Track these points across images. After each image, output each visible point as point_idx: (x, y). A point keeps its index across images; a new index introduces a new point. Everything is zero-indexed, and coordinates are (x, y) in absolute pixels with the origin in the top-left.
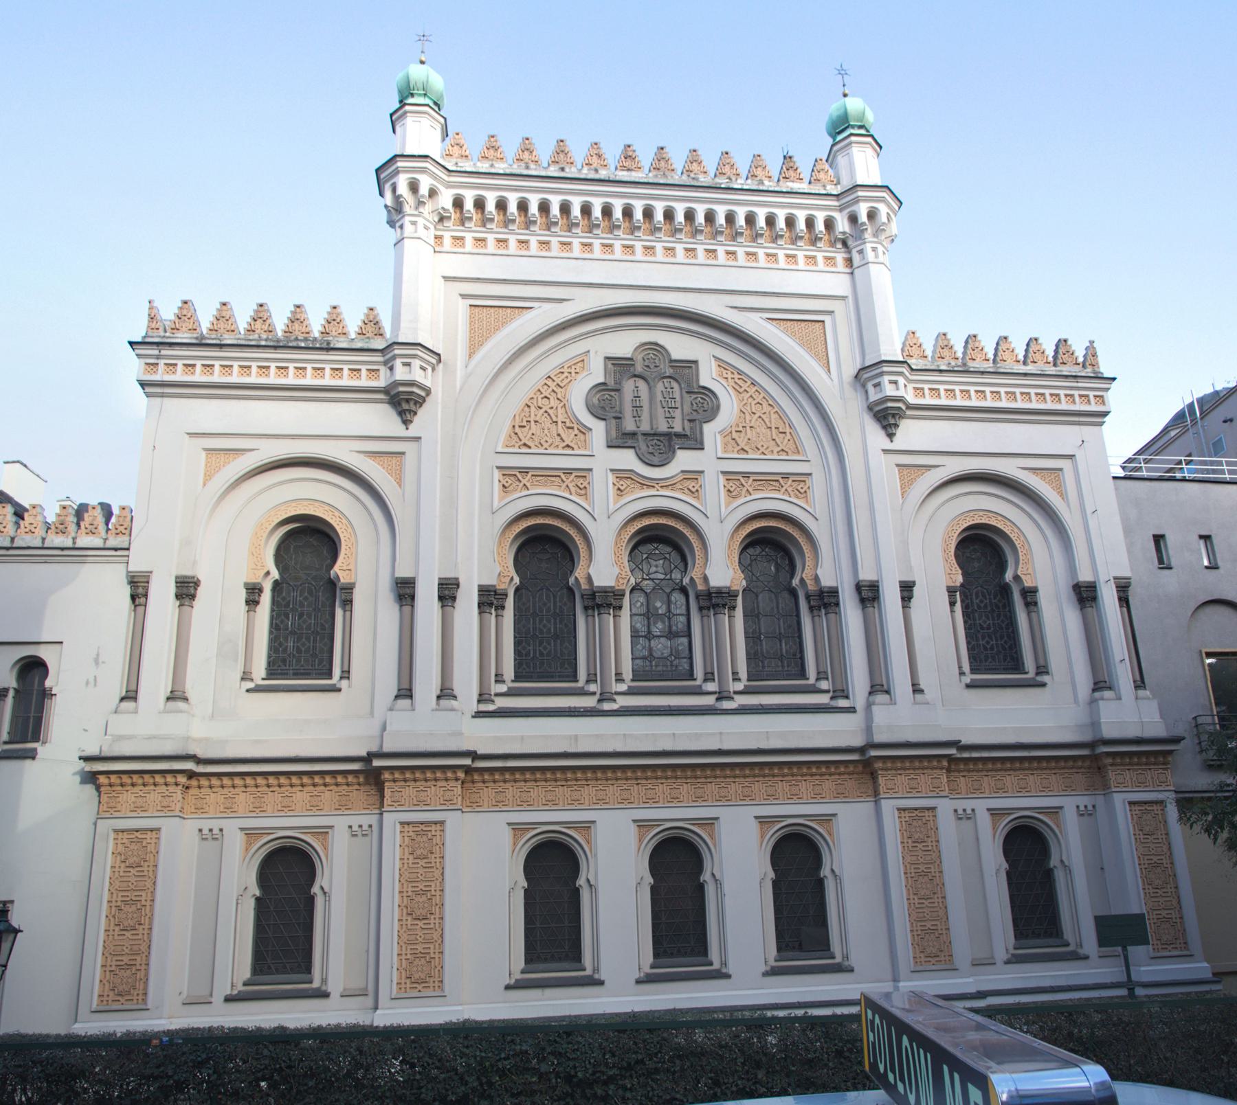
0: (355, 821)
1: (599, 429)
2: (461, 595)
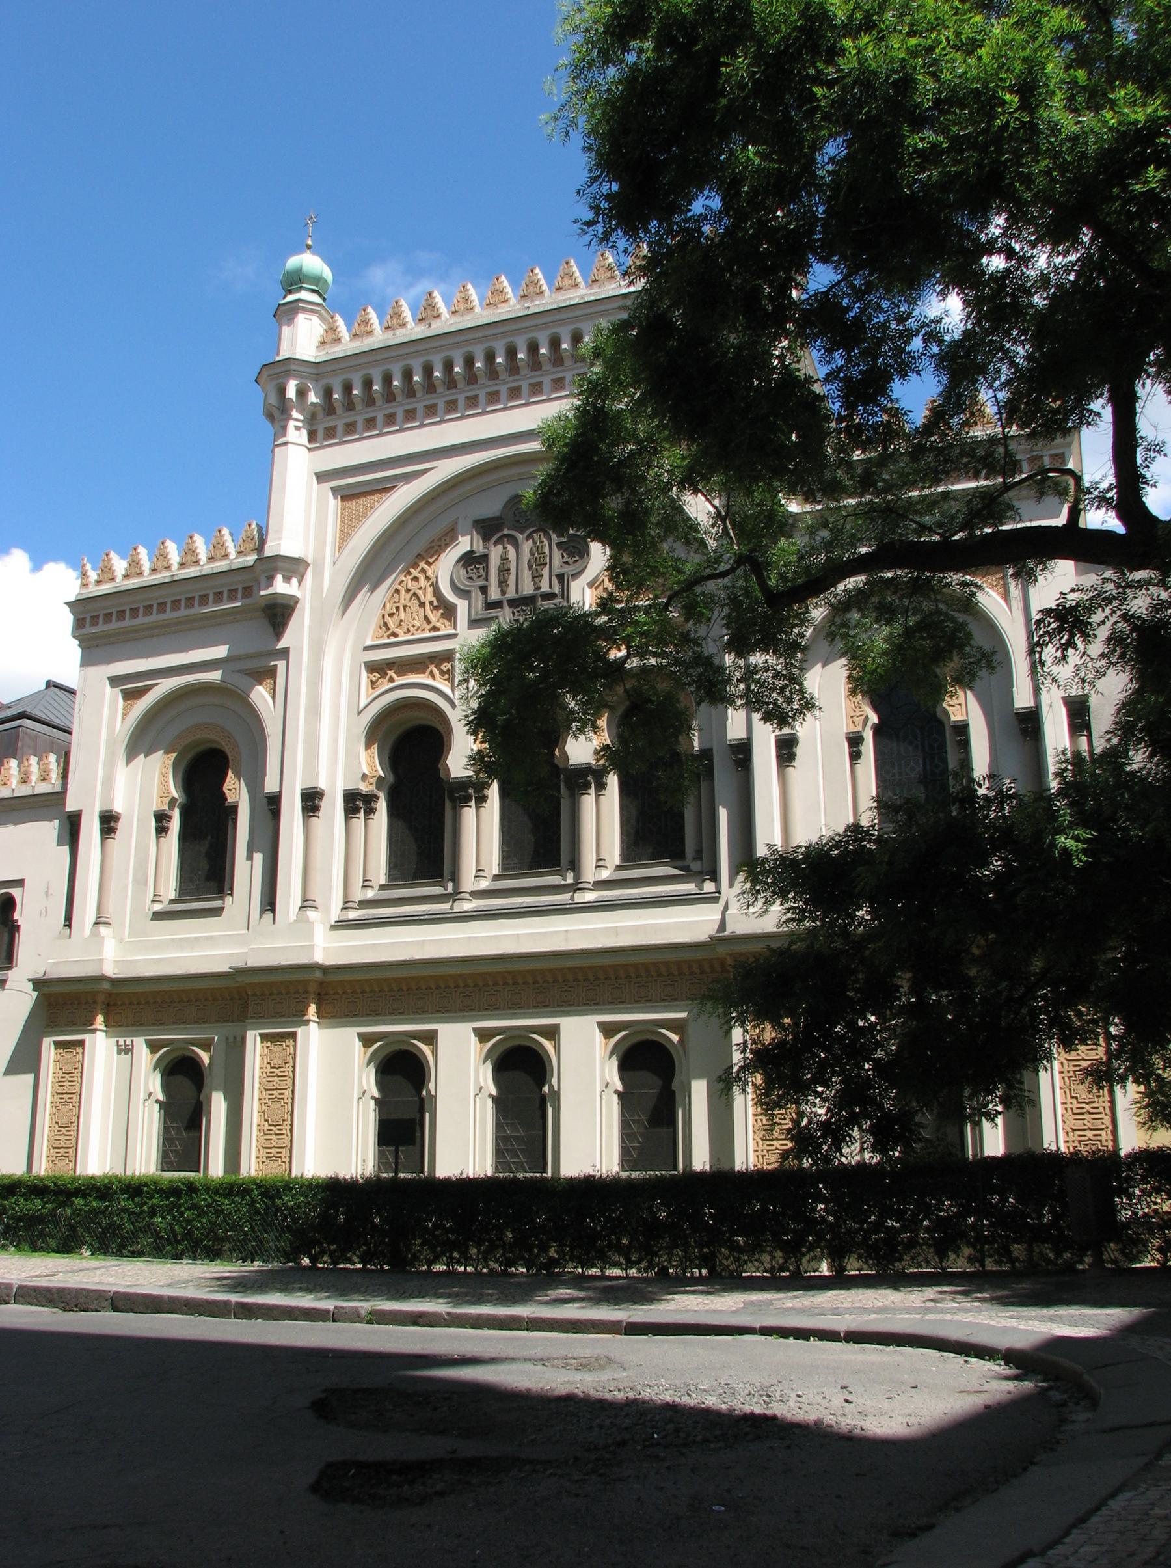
1: (462, 606)
2: (324, 804)
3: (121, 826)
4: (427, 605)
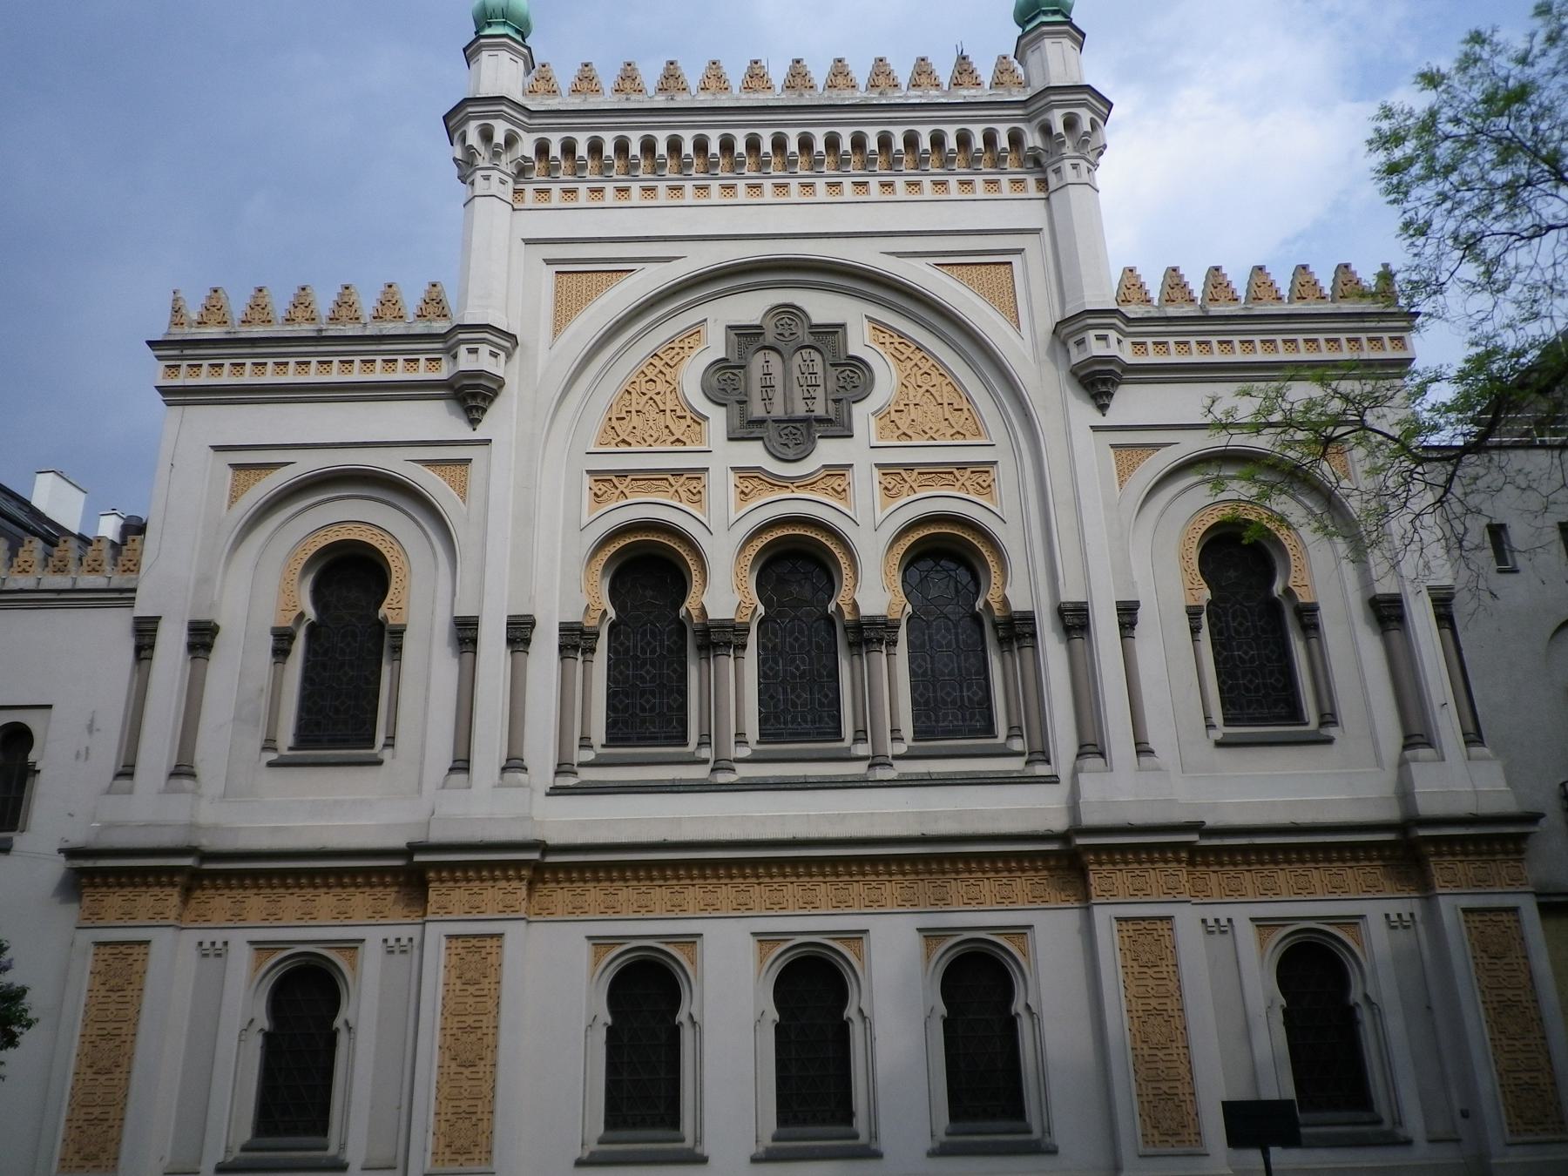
0: (392, 933)
1: (718, 419)
2: (537, 637)
3: (219, 640)
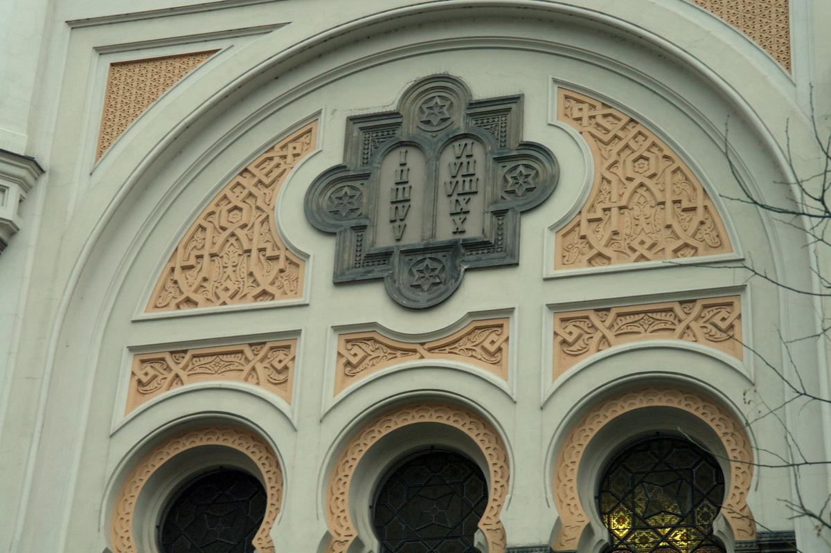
1: (321, 254)
4: (254, 253)
